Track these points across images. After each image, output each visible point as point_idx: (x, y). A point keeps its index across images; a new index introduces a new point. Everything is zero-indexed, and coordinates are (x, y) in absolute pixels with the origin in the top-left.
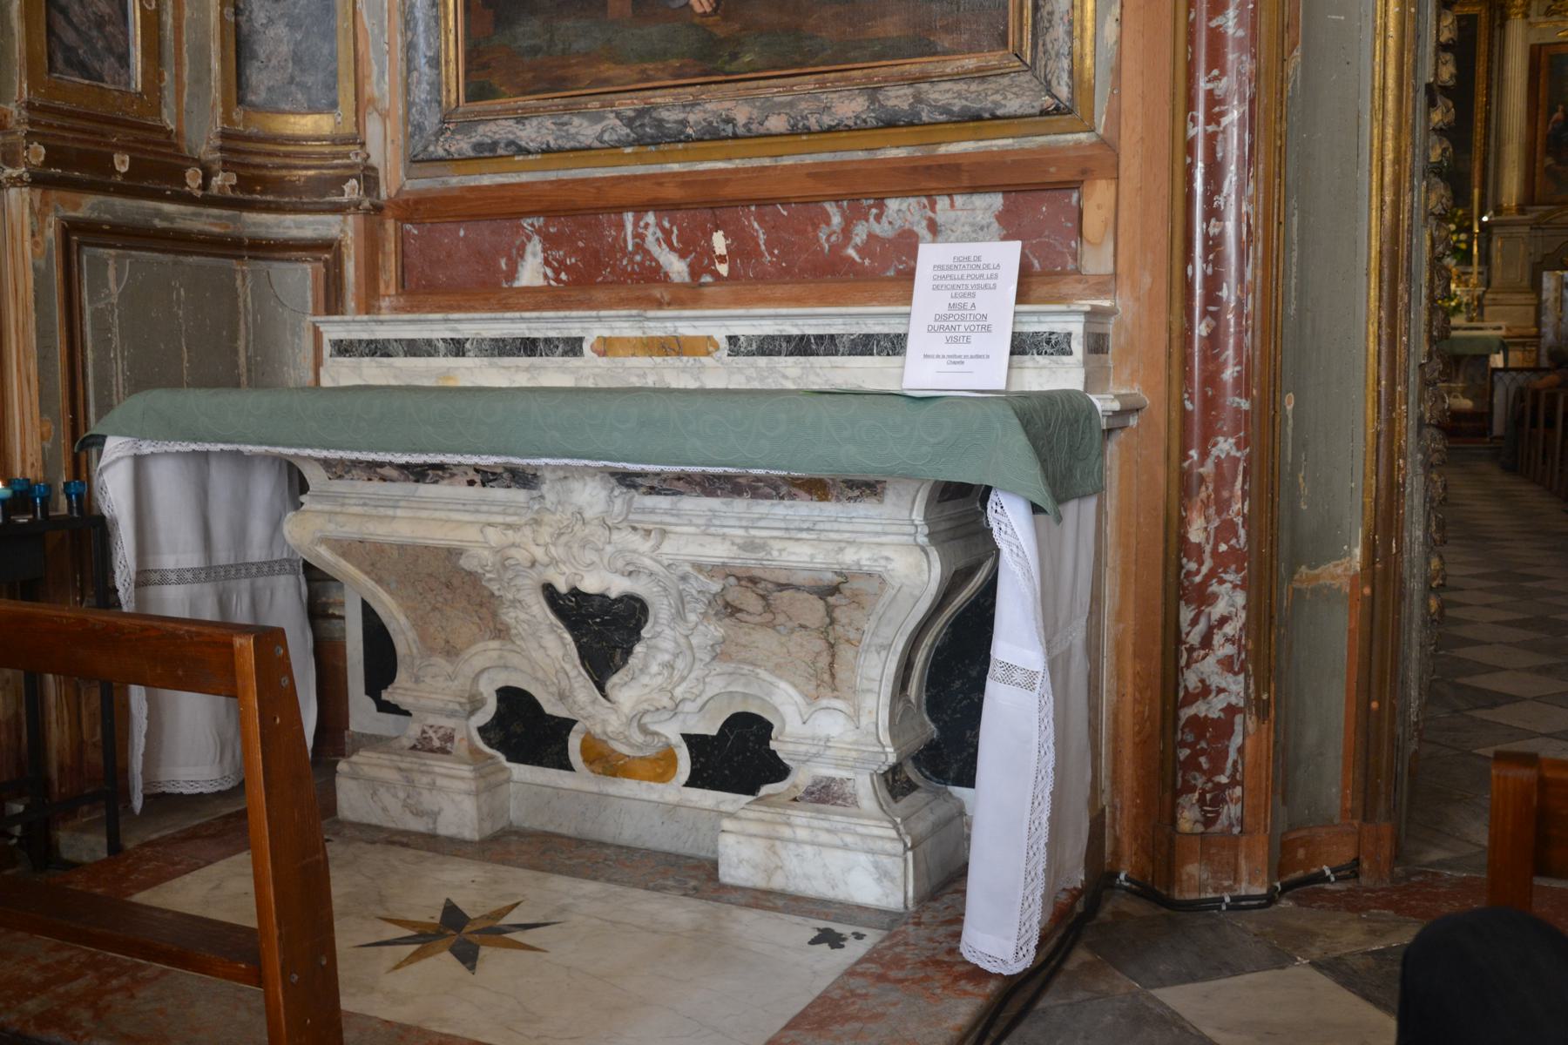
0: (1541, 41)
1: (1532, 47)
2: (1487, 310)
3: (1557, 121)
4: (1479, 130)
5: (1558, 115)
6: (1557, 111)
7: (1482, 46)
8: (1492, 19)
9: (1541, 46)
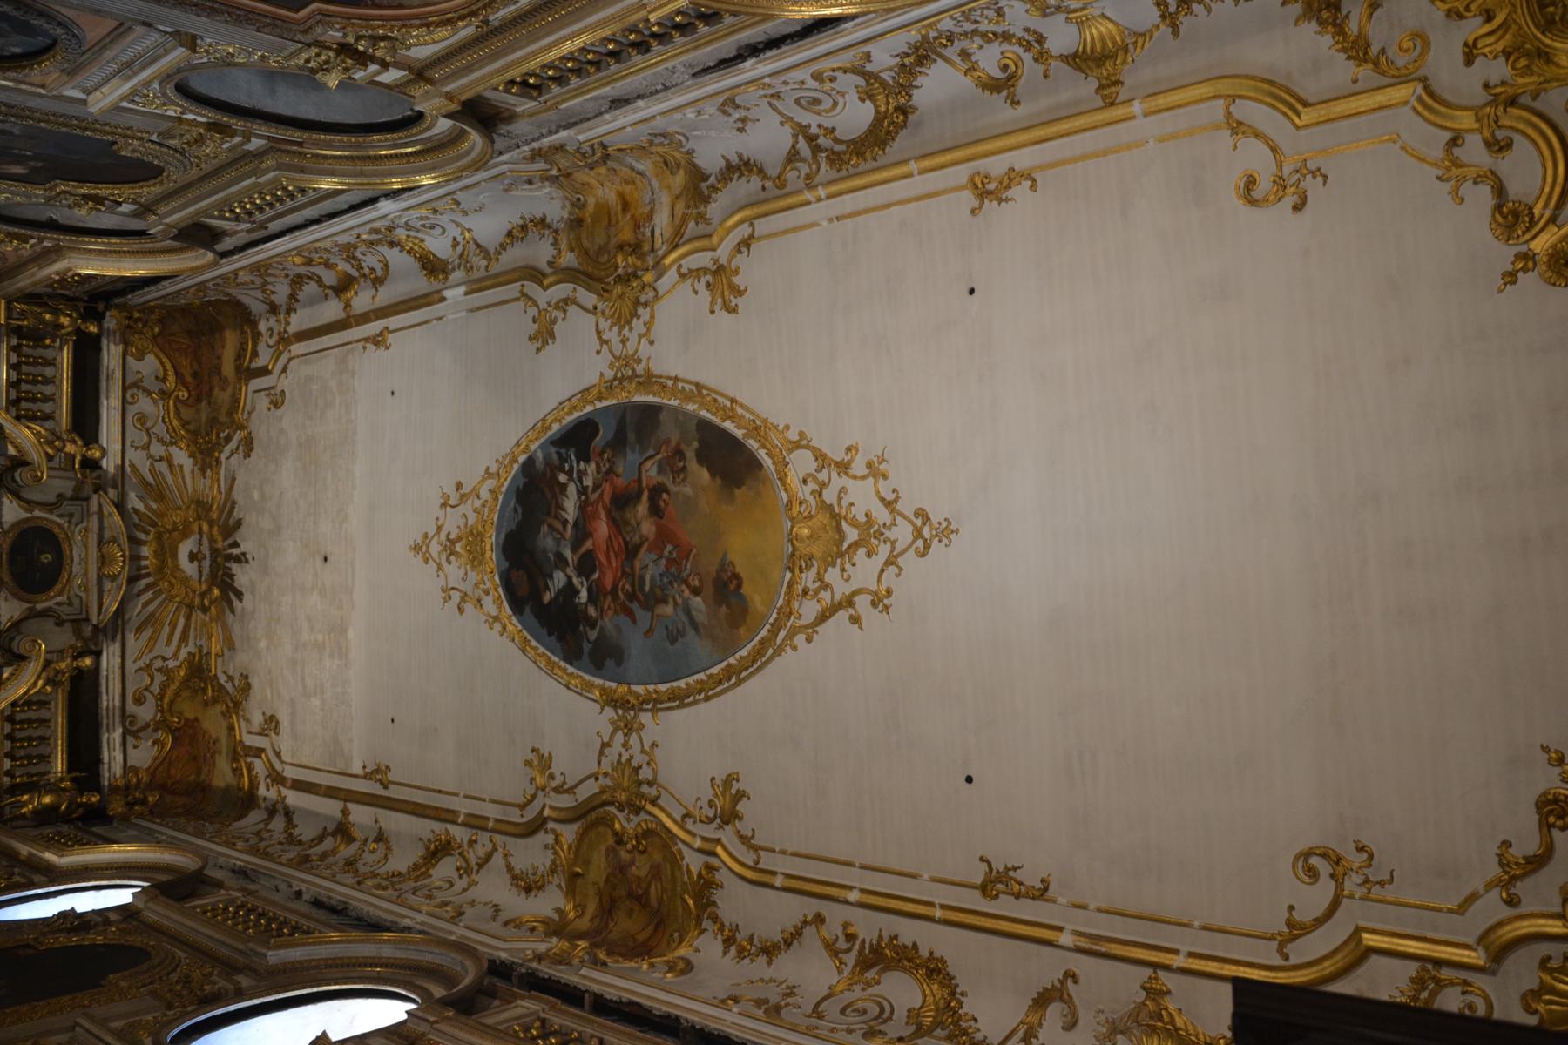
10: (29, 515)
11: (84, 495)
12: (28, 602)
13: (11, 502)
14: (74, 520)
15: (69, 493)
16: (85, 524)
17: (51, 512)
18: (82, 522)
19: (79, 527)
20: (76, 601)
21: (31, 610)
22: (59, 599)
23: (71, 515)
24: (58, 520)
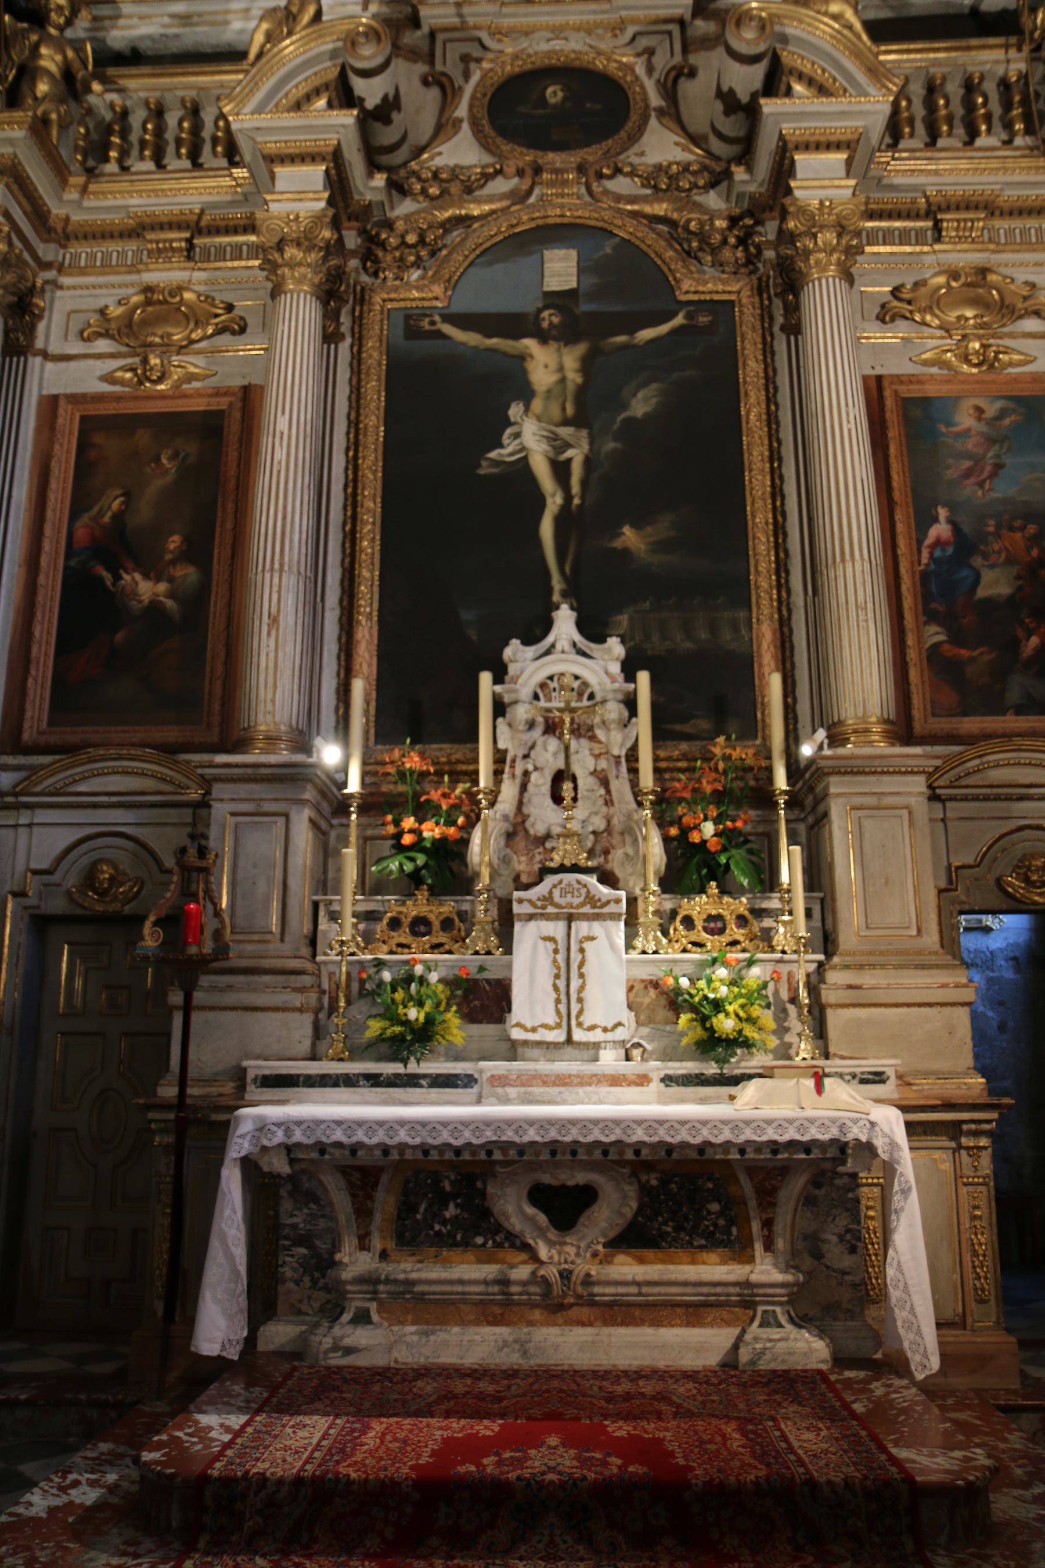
0: (878, 371)
1: (865, 379)
2: (835, 1019)
3: (938, 543)
4: (762, 548)
5: (940, 530)
6: (936, 520)
7: (752, 364)
8: (766, 315)
9: (879, 378)
10: (465, 126)
11: (425, 46)
12: (645, 119)
13: (440, 154)
14: (477, 53)
15: (422, 68)
16: (484, 35)
17: (457, 92)
18: (480, 41)
19: (488, 42)
20: (643, 42)
21: (661, 112)
22: (640, 70)
23: (465, 59)
24: (475, 78)
